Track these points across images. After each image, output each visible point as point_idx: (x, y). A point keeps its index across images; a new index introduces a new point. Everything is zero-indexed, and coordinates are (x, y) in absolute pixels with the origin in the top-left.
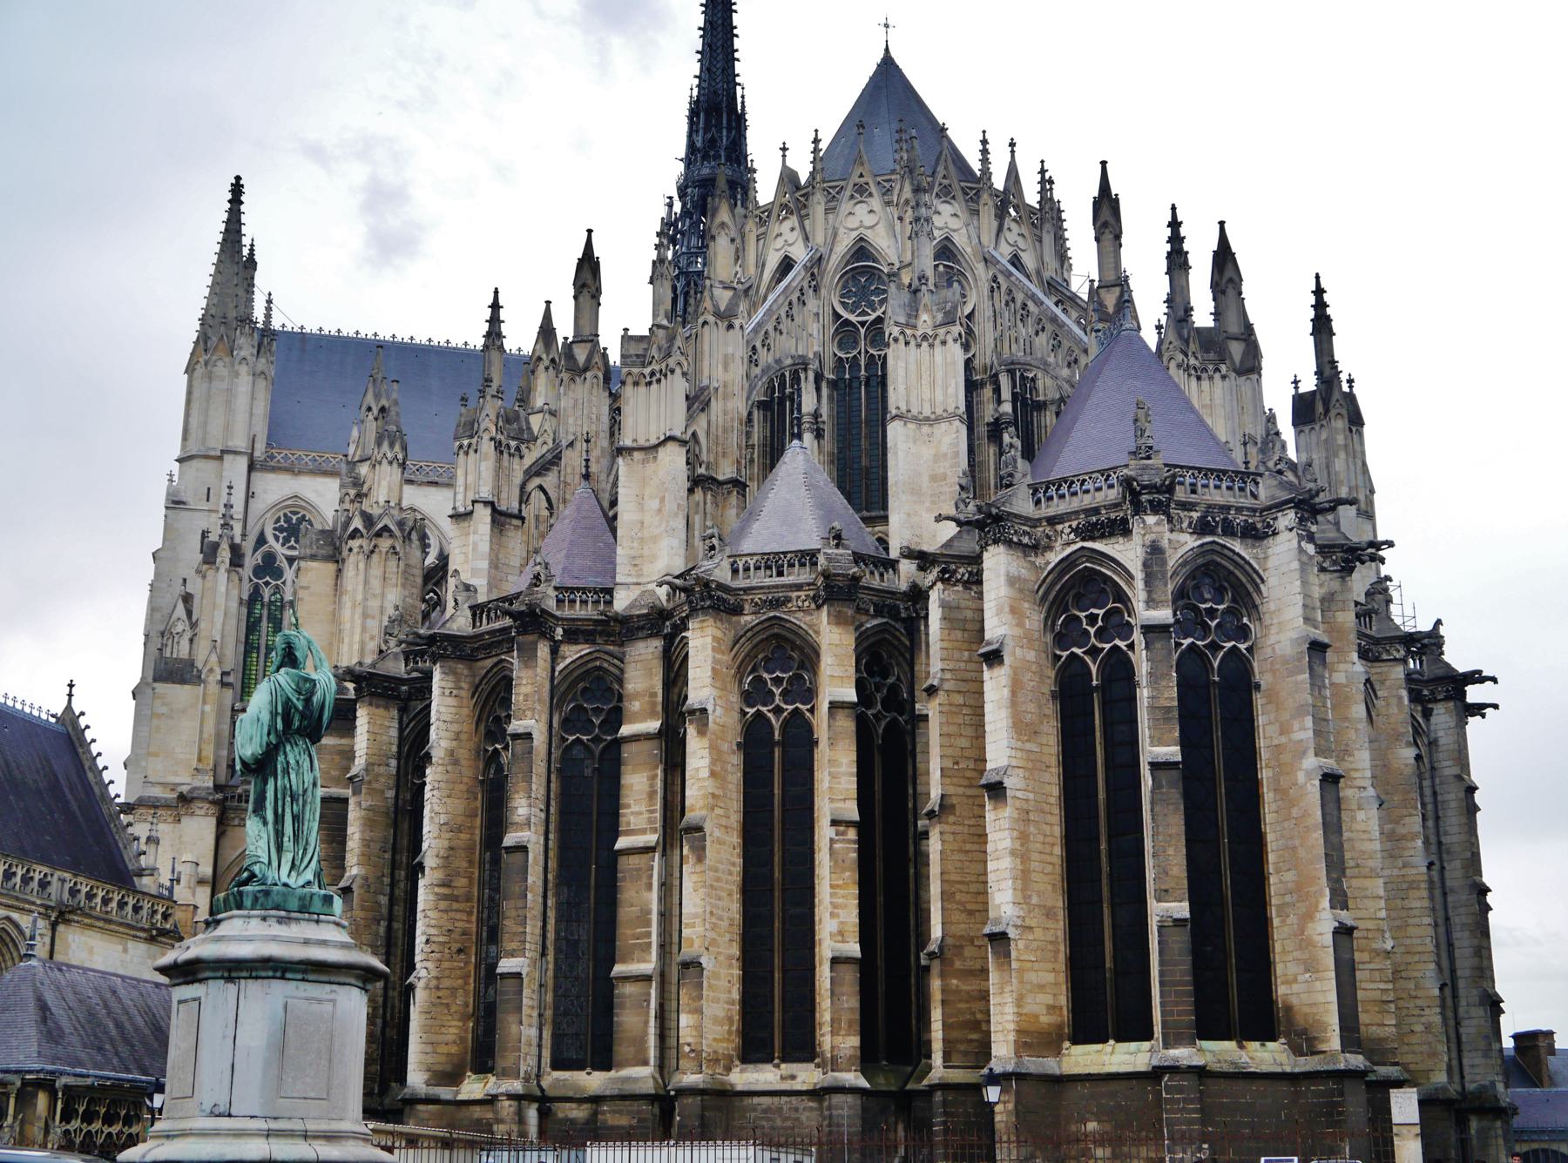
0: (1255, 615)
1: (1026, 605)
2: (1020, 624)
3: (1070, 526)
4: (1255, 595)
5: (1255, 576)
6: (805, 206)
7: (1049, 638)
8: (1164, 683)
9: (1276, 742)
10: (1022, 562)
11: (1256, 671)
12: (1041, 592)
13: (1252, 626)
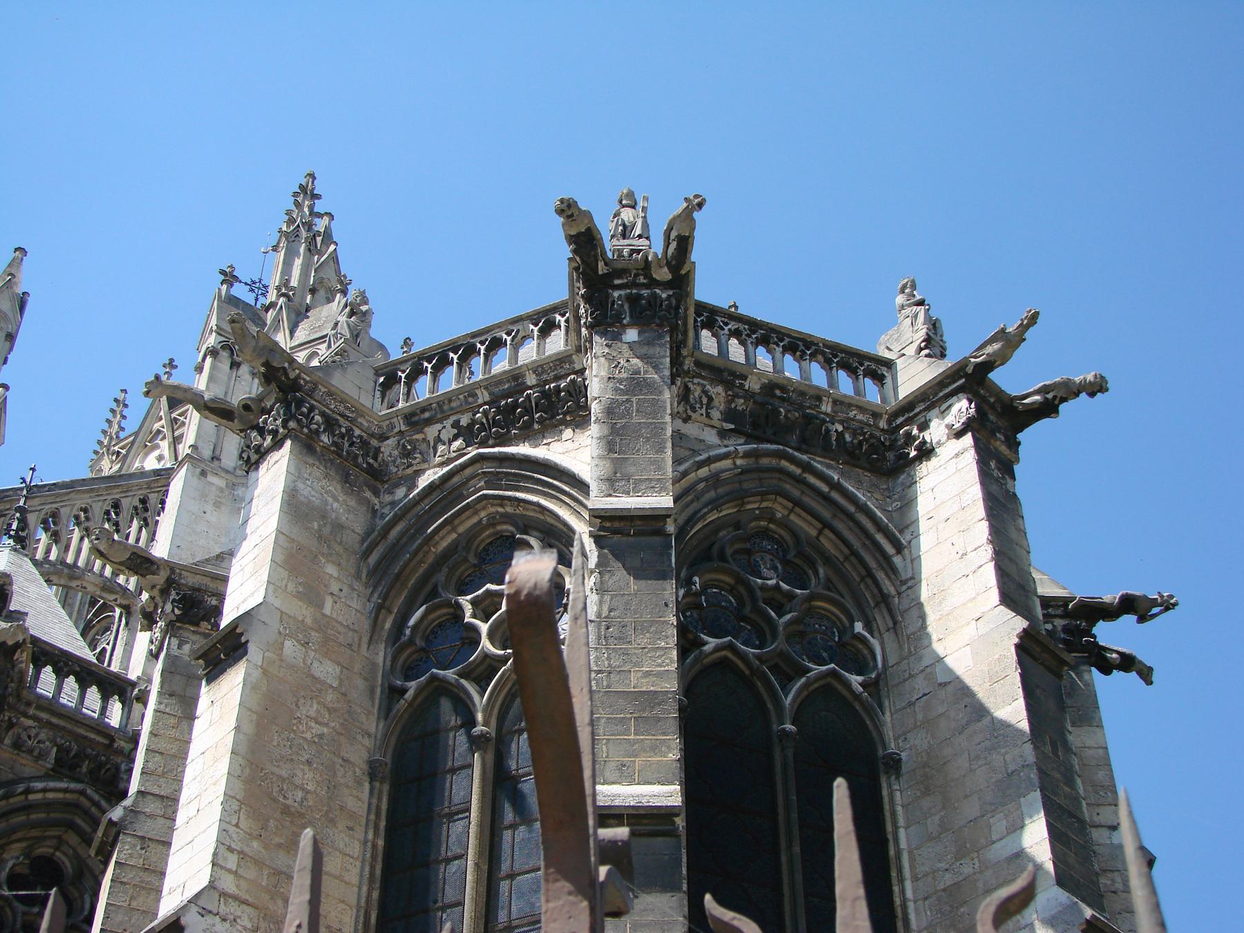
0: (881, 620)
1: (331, 570)
2: (312, 595)
3: (456, 424)
4: (880, 576)
5: (880, 538)
6: (183, 424)
7: (381, 655)
8: (643, 640)
9: (948, 879)
10: (335, 487)
11: (889, 734)
12: (373, 558)
13: (875, 643)
